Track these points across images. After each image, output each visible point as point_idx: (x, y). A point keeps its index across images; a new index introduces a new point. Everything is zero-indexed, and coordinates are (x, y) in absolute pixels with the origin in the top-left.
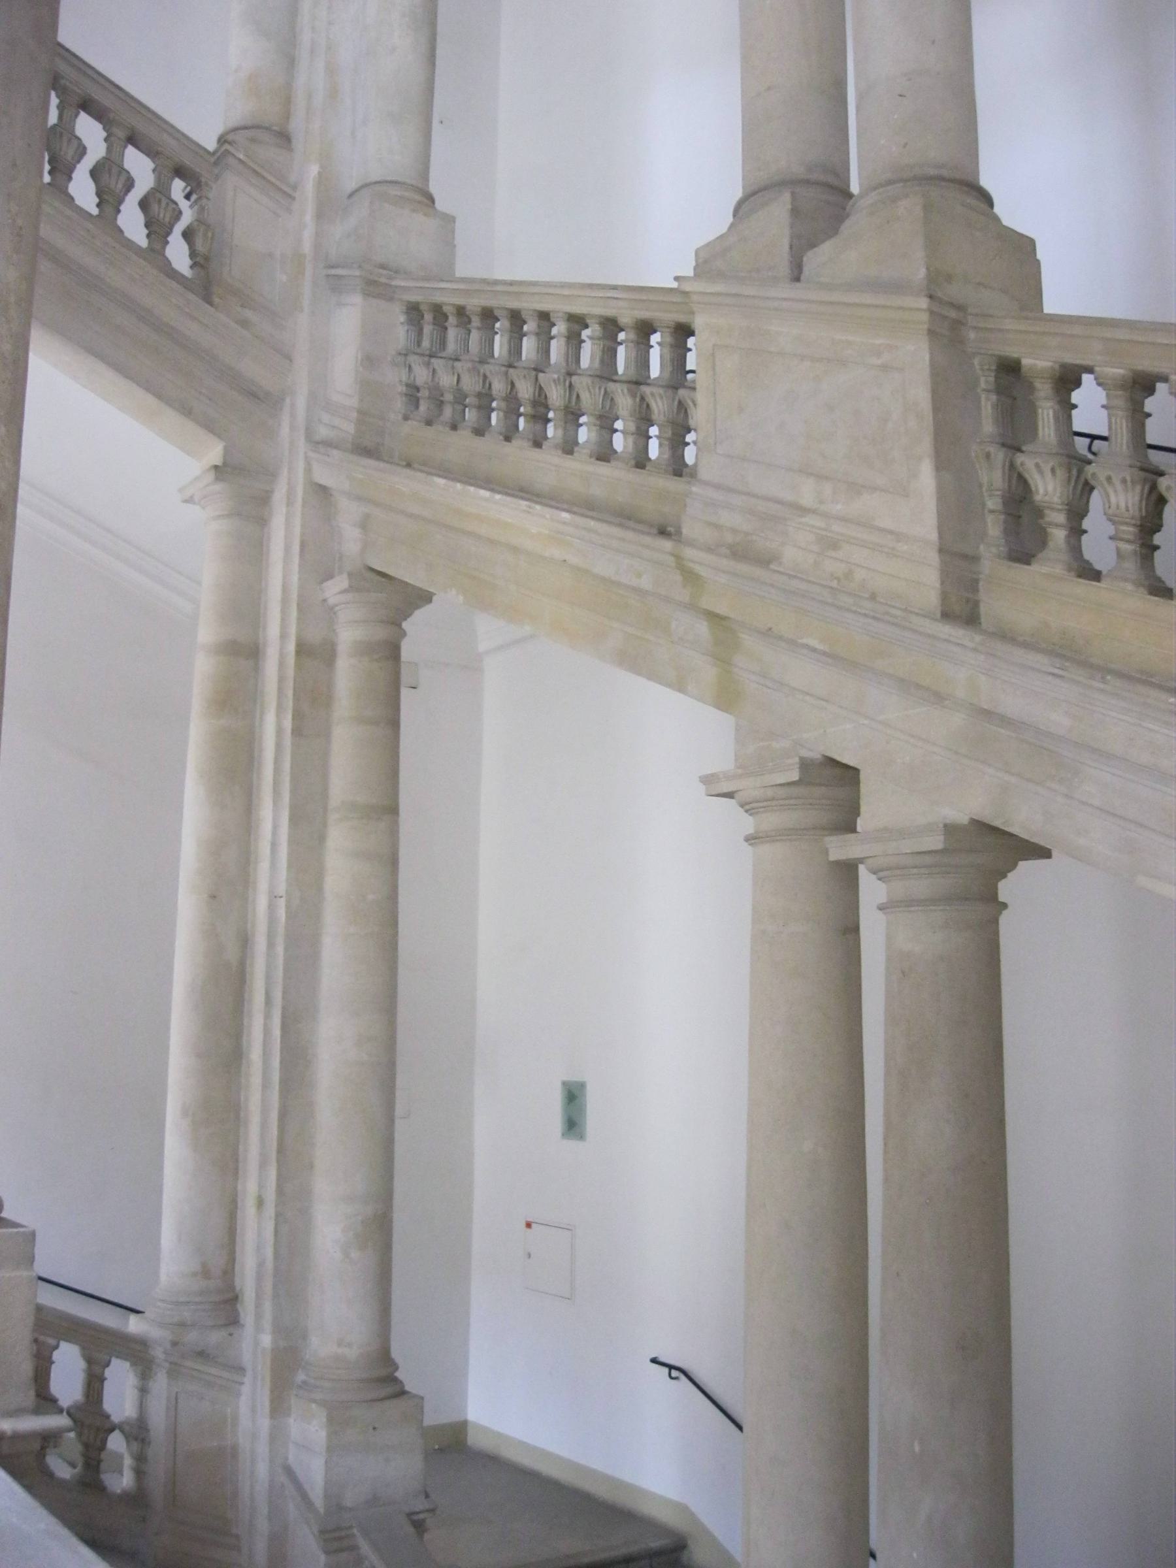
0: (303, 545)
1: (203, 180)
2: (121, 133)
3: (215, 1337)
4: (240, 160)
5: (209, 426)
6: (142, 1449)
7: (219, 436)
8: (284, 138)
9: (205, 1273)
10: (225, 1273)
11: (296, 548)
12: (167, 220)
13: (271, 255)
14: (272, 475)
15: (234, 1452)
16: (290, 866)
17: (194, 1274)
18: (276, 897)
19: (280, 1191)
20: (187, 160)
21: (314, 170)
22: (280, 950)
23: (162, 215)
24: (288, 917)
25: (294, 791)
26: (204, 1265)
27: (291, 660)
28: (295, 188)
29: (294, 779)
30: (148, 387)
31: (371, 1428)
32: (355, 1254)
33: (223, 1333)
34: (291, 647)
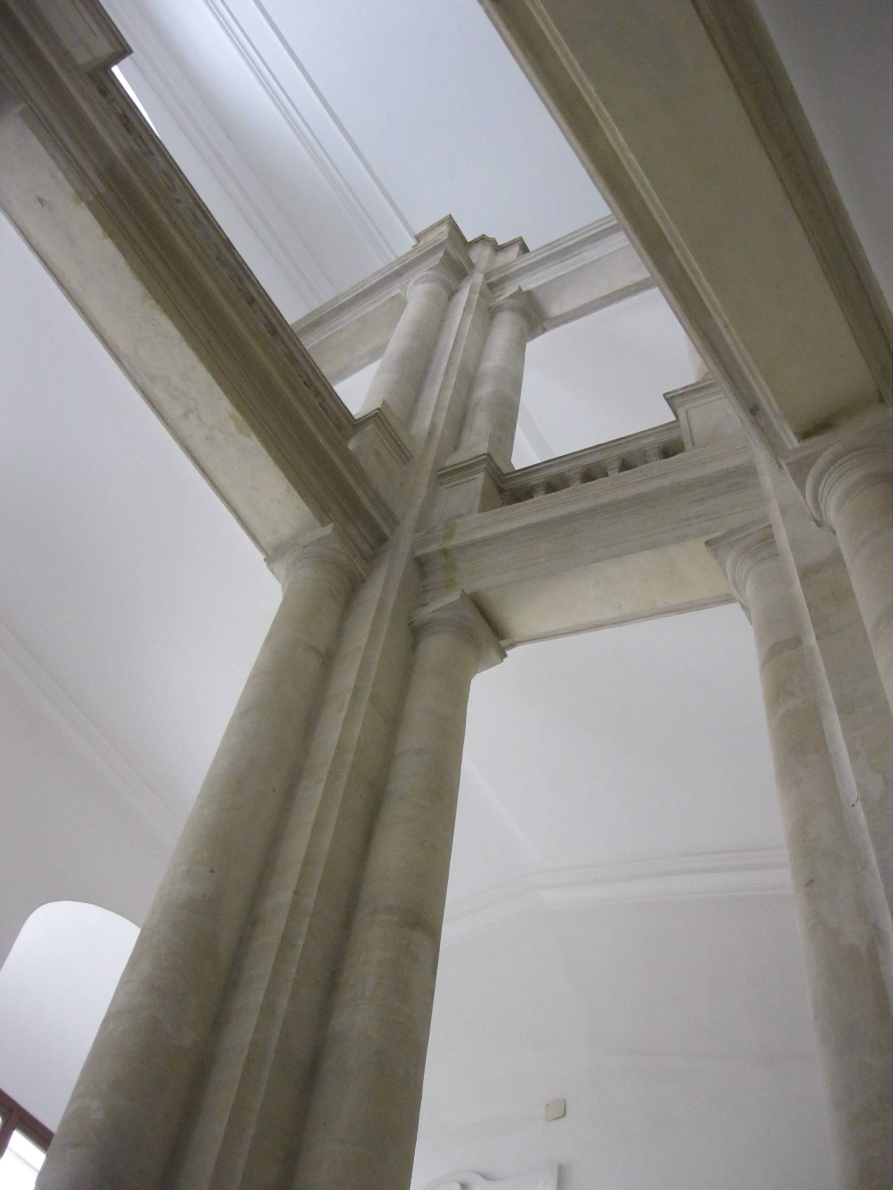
16: (854, 755)
18: (853, 806)
20: (666, 437)
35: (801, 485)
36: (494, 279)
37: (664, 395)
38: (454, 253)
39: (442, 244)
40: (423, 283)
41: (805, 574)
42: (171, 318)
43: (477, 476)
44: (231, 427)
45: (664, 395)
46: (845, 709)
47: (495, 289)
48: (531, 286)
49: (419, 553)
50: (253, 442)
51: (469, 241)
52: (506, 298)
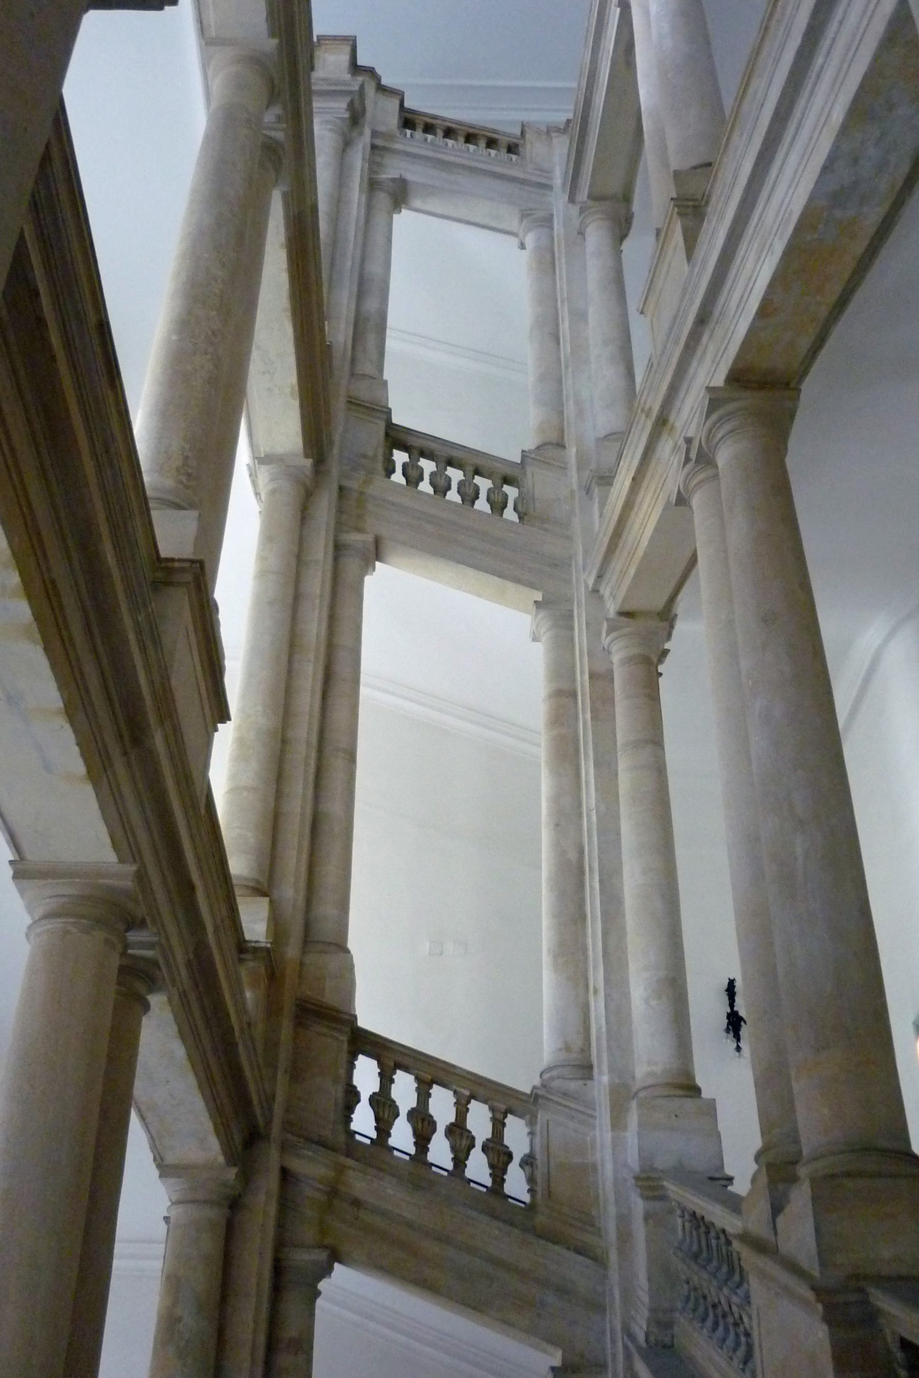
0: (587, 624)
1: (519, 478)
2: (470, 469)
3: (573, 1086)
4: (534, 459)
5: (532, 585)
6: (532, 1172)
7: (537, 589)
8: (561, 445)
9: (567, 1048)
10: (582, 1051)
11: (584, 627)
12: (496, 499)
13: (559, 499)
14: (570, 601)
15: (594, 1168)
16: (597, 790)
17: (560, 1050)
19: (607, 981)
20: (508, 471)
21: (574, 450)
22: (595, 838)
23: (496, 499)
24: (598, 819)
25: (596, 752)
26: (566, 1043)
27: (587, 684)
28: (566, 464)
29: (596, 745)
30: (494, 573)
31: (673, 1115)
32: (653, 1003)
33: (581, 1083)
34: (587, 676)
35: (607, 635)
36: (379, 142)
37: (523, 451)
38: (357, 104)
39: (351, 92)
40: (331, 130)
41: (592, 676)
42: (295, 326)
43: (378, 421)
44: (288, 390)
45: (523, 451)
46: (597, 765)
47: (377, 152)
48: (409, 177)
49: (346, 483)
50: (295, 404)
51: (359, 63)
52: (387, 179)
